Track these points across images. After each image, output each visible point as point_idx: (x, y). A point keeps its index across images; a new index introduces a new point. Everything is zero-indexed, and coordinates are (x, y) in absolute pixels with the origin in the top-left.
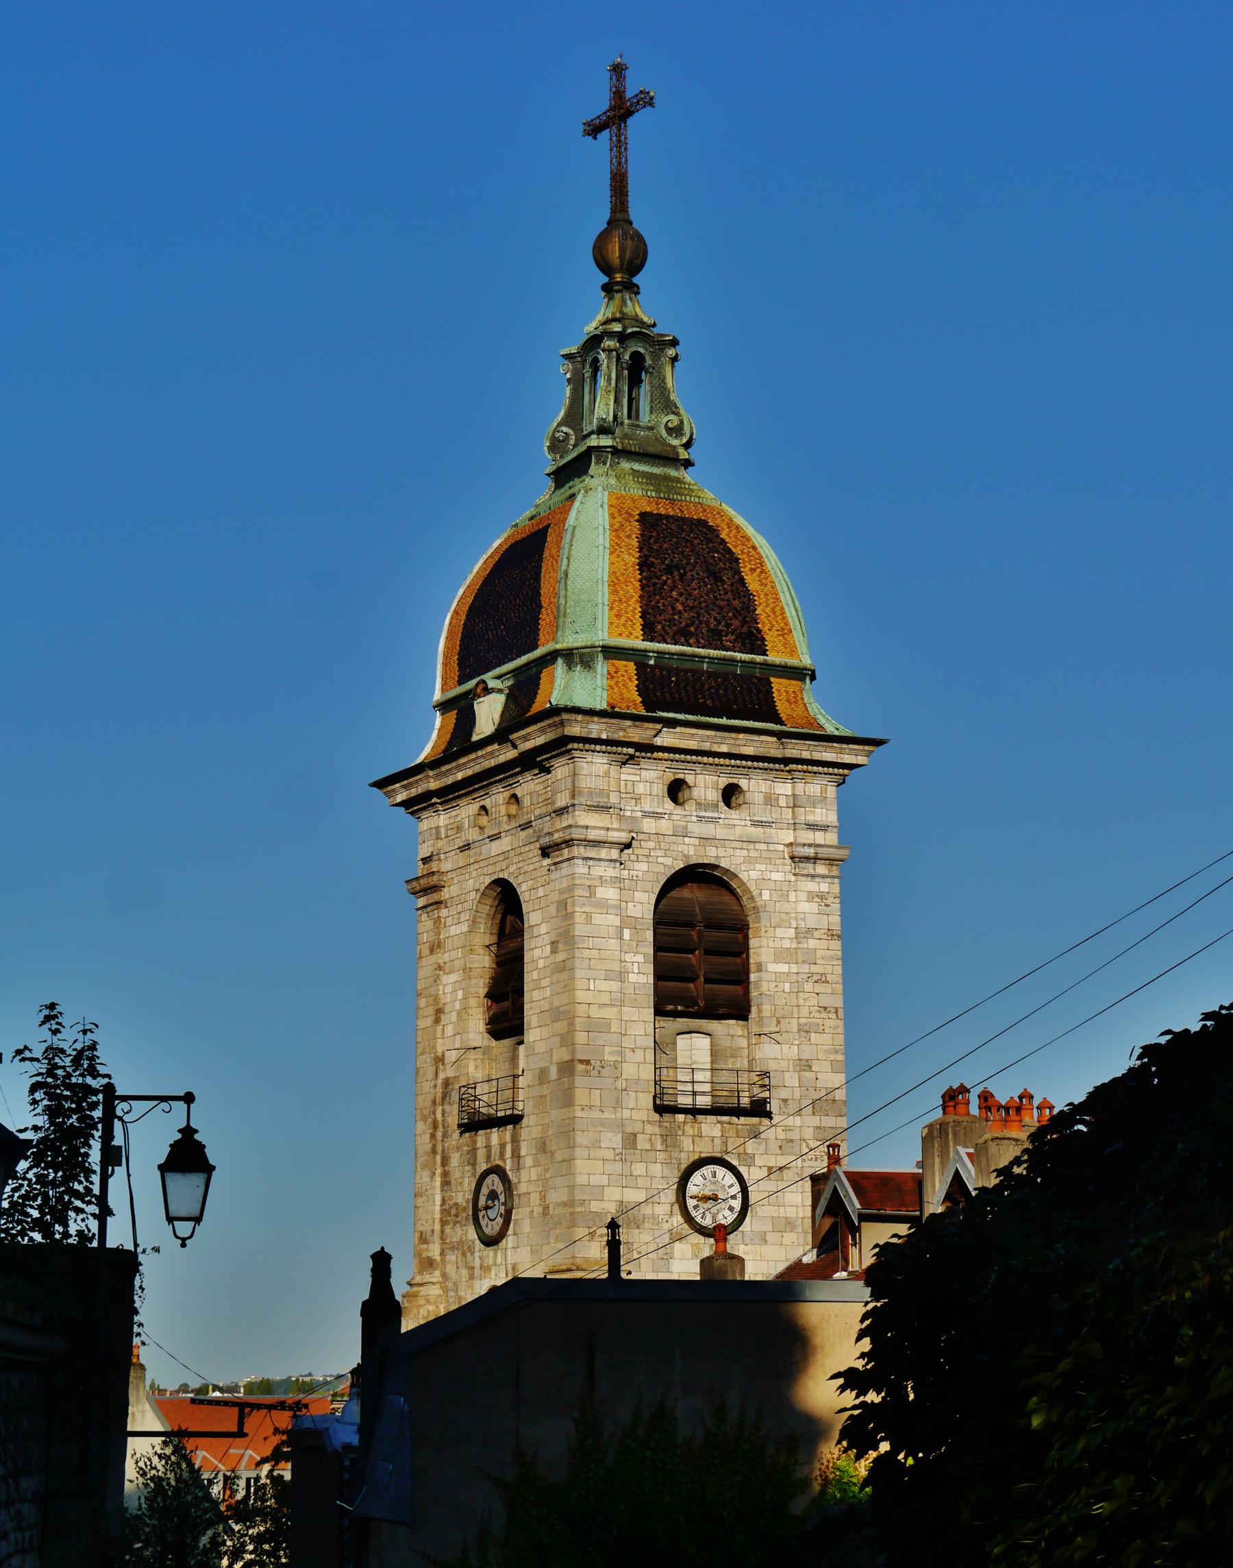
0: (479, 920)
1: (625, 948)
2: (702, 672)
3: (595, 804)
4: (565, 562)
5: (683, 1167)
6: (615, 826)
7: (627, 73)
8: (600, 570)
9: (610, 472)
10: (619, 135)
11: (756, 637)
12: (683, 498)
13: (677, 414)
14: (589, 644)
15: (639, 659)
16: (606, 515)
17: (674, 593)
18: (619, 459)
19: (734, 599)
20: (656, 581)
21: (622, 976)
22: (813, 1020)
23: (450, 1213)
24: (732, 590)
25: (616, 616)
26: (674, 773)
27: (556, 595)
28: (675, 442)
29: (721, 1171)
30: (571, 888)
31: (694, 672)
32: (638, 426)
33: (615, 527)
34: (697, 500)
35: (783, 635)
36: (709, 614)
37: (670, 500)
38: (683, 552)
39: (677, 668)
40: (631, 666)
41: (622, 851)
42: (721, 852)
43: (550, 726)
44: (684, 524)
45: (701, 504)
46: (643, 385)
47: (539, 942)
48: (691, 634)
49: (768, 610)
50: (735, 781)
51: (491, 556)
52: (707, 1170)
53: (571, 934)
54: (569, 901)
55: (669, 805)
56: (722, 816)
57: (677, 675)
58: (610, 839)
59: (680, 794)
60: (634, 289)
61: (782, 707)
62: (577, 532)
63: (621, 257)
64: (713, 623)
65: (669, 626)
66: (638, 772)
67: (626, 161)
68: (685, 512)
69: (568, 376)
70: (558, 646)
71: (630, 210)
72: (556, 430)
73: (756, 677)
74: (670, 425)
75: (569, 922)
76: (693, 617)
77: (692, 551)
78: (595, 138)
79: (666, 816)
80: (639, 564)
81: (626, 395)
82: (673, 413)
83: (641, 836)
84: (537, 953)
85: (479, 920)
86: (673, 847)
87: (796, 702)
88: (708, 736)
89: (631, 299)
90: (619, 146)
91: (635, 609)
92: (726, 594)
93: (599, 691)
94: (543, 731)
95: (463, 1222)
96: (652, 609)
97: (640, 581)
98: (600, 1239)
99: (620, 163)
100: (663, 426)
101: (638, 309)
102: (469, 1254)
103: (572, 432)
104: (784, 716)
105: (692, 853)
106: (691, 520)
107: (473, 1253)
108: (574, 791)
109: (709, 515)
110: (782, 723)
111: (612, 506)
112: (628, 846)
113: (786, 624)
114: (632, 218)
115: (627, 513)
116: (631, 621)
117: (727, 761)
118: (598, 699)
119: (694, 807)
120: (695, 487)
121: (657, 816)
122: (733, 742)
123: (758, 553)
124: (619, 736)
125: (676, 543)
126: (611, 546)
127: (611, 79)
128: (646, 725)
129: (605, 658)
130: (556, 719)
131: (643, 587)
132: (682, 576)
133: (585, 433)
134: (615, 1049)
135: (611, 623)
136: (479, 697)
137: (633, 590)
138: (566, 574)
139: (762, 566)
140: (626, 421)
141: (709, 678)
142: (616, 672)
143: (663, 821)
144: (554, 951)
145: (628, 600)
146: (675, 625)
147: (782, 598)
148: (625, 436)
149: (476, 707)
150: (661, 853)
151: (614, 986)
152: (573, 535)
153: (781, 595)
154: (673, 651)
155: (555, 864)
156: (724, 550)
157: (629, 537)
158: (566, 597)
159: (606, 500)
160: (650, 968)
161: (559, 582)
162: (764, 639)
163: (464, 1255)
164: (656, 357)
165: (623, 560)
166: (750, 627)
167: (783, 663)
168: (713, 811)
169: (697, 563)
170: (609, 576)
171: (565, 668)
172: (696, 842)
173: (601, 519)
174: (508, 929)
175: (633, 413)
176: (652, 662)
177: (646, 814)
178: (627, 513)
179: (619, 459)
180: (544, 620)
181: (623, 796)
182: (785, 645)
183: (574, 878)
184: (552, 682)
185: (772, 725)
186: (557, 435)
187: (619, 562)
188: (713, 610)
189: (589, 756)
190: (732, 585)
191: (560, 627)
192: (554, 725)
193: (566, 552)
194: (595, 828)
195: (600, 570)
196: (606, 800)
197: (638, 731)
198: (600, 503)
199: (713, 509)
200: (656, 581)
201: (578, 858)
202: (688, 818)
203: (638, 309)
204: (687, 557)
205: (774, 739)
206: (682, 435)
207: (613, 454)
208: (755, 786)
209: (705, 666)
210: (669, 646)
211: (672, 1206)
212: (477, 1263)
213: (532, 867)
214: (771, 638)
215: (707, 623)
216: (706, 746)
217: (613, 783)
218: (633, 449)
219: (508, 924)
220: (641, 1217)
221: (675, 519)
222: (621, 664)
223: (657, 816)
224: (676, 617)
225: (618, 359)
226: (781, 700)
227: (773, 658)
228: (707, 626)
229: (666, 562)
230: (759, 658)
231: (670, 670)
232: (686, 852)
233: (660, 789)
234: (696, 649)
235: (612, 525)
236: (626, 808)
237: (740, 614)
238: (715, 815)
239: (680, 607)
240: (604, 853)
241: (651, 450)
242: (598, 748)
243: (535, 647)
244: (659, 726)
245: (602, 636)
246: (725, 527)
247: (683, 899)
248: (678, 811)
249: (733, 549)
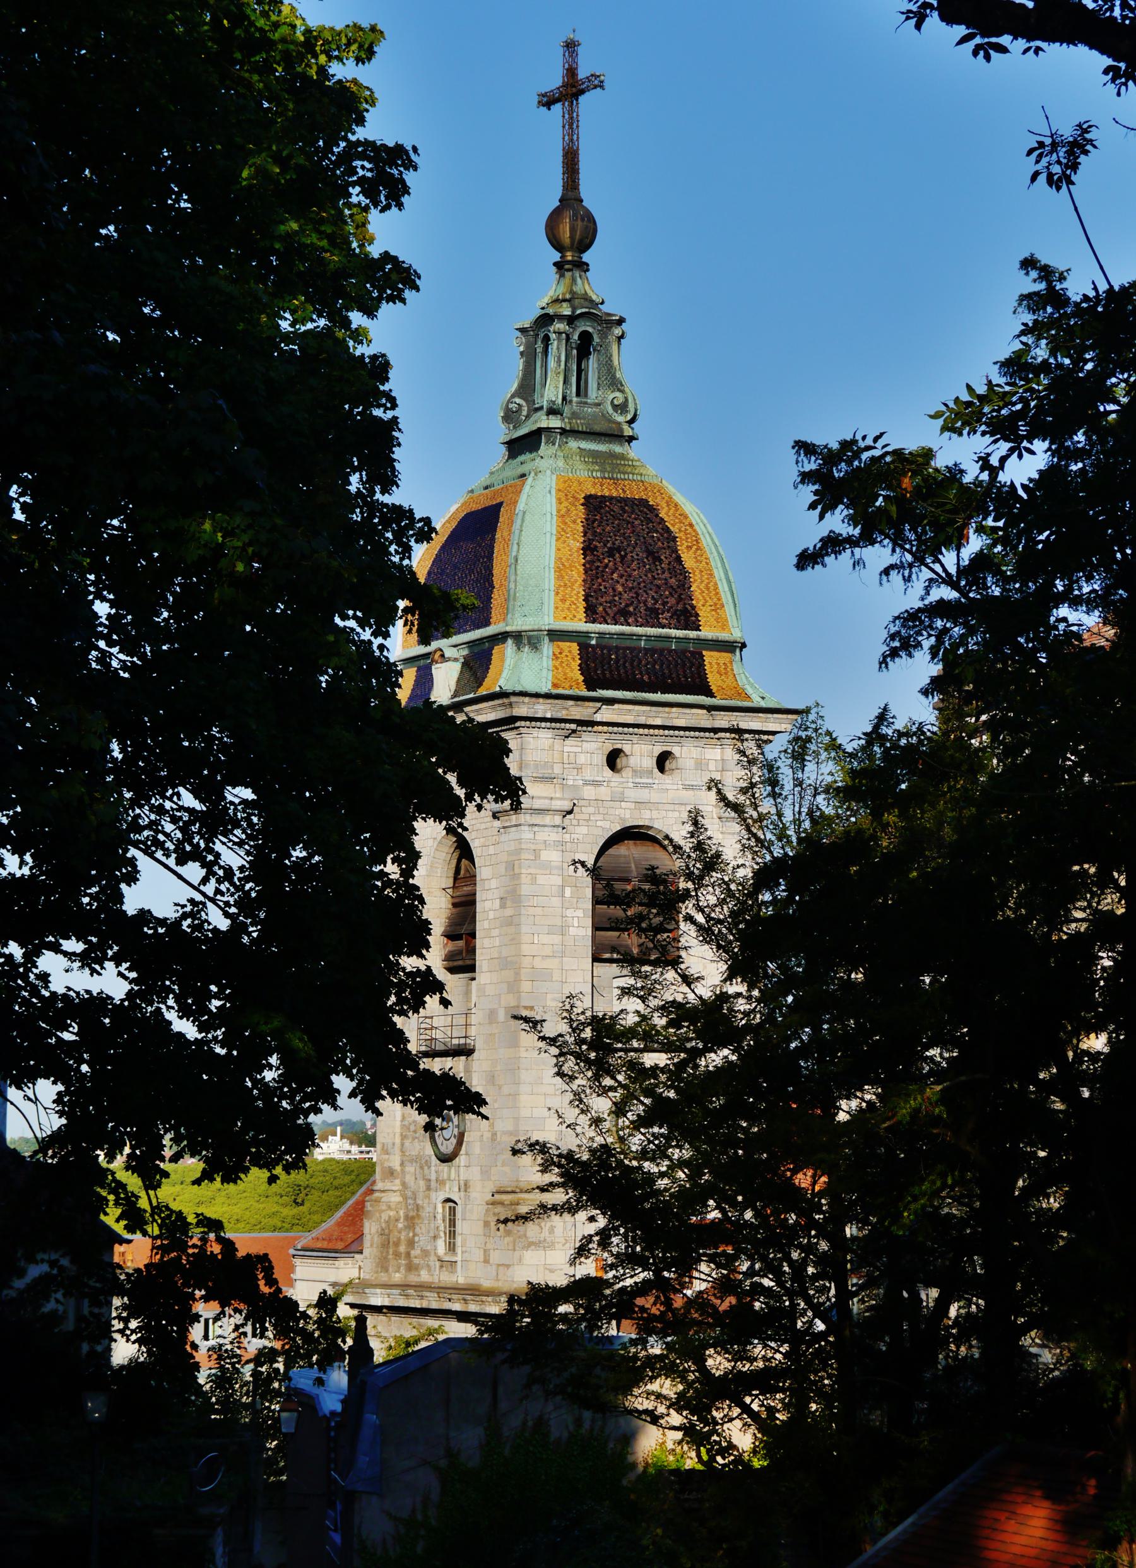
0: (437, 865)
1: (566, 905)
2: (640, 649)
3: (541, 776)
4: (515, 547)
6: (558, 795)
7: (580, 49)
8: (547, 557)
9: (558, 453)
10: (571, 112)
11: (690, 613)
12: (626, 476)
13: (622, 392)
14: (536, 627)
15: (582, 640)
16: (554, 500)
17: (615, 575)
18: (567, 438)
19: (671, 578)
20: (599, 564)
21: (563, 930)
23: (409, 1129)
24: (669, 569)
25: (561, 600)
26: (613, 744)
27: (507, 578)
28: (620, 419)
30: (519, 851)
31: (632, 649)
32: (586, 403)
33: (562, 512)
34: (639, 478)
35: (715, 610)
36: (647, 594)
37: (614, 479)
38: (624, 534)
39: (616, 646)
40: (575, 647)
41: (564, 816)
42: (655, 814)
43: (500, 705)
44: (626, 505)
45: (642, 482)
46: (591, 357)
47: (490, 895)
48: (630, 614)
49: (702, 586)
50: (668, 749)
51: (448, 521)
53: (518, 893)
54: (516, 862)
55: (608, 772)
56: (656, 781)
57: (616, 654)
58: (553, 808)
59: (618, 760)
60: (583, 267)
61: (713, 680)
62: (527, 517)
63: (572, 237)
64: (650, 602)
65: (610, 607)
66: (580, 744)
67: (578, 138)
68: (628, 492)
69: (522, 349)
70: (508, 629)
71: (580, 187)
72: (510, 401)
73: (690, 652)
74: (616, 402)
75: (516, 882)
76: (632, 597)
77: (633, 532)
78: (549, 109)
79: (605, 784)
80: (583, 549)
81: (575, 374)
82: (619, 390)
83: (582, 803)
84: (488, 904)
85: (437, 865)
86: (611, 811)
87: (726, 673)
89: (580, 276)
90: (571, 124)
91: (579, 593)
92: (663, 573)
93: (545, 672)
94: (493, 708)
95: (421, 1138)
96: (595, 592)
97: (584, 565)
99: (571, 140)
100: (609, 403)
101: (587, 287)
102: (426, 1168)
103: (524, 403)
104: (714, 688)
105: (628, 816)
106: (633, 500)
107: (429, 1167)
108: (521, 764)
109: (650, 494)
110: (710, 694)
111: (559, 490)
112: (570, 812)
113: (719, 599)
114: (583, 195)
115: (574, 497)
116: (575, 604)
117: (661, 732)
118: (544, 680)
119: (630, 774)
120: (638, 464)
121: (596, 784)
122: (666, 715)
123: (695, 531)
124: (563, 714)
125: (618, 525)
126: (558, 532)
127: (564, 55)
128: (587, 704)
129: (551, 640)
130: (506, 701)
131: (586, 572)
132: (623, 558)
133: (537, 406)
134: (556, 995)
135: (557, 608)
136: (437, 663)
137: (577, 575)
138: (516, 560)
139: (698, 543)
140: (575, 399)
141: (646, 654)
142: (560, 653)
143: (602, 788)
144: (503, 906)
145: (573, 585)
146: (615, 606)
147: (716, 574)
148: (574, 415)
149: (434, 671)
150: (600, 817)
151: (557, 939)
152: (523, 521)
153: (715, 571)
154: (613, 631)
155: (504, 828)
156: (663, 529)
157: (574, 522)
158: (515, 581)
159: (554, 485)
160: (589, 922)
161: (510, 566)
162: (697, 615)
163: (422, 1168)
164: (604, 335)
165: (568, 546)
166: (685, 604)
167: (714, 638)
168: (648, 778)
169: (637, 544)
170: (556, 563)
171: (515, 648)
172: (632, 806)
173: (548, 505)
174: (462, 872)
175: (582, 392)
176: (593, 642)
177: (586, 783)
178: (574, 497)
179: (567, 438)
180: (496, 600)
181: (566, 766)
182: (717, 620)
183: (520, 843)
184: (503, 660)
185: (703, 697)
186: (511, 406)
187: (564, 548)
188: (651, 589)
189: (535, 732)
190: (669, 563)
191: (510, 610)
192: (503, 705)
193: (516, 538)
194: (539, 798)
195: (547, 557)
196: (550, 771)
197: (579, 709)
198: (548, 489)
199: (653, 486)
200: (599, 564)
201: (524, 825)
202: (625, 785)
203: (587, 287)
204: (628, 539)
205: (705, 711)
206: (627, 411)
207: (561, 434)
208: (686, 752)
209: (643, 643)
210: (610, 626)
212: (433, 1177)
213: (483, 826)
214: (705, 614)
215: (645, 602)
216: (642, 720)
217: (556, 755)
218: (580, 429)
219: (463, 867)
221: (619, 500)
222: (565, 645)
223: (596, 784)
224: (617, 598)
225: (568, 338)
226: (712, 672)
227: (706, 633)
228: (645, 605)
229: (609, 545)
230: (692, 634)
231: (610, 649)
232: (622, 816)
233: (602, 759)
234: (635, 628)
235: (559, 511)
236: (569, 777)
237: (676, 592)
238: (650, 781)
239: (620, 588)
240: (547, 819)
241: (597, 428)
242: (543, 724)
243: (487, 623)
244: (598, 705)
245: (549, 621)
246: (665, 505)
247: (619, 856)
248: (614, 778)
249: (671, 528)
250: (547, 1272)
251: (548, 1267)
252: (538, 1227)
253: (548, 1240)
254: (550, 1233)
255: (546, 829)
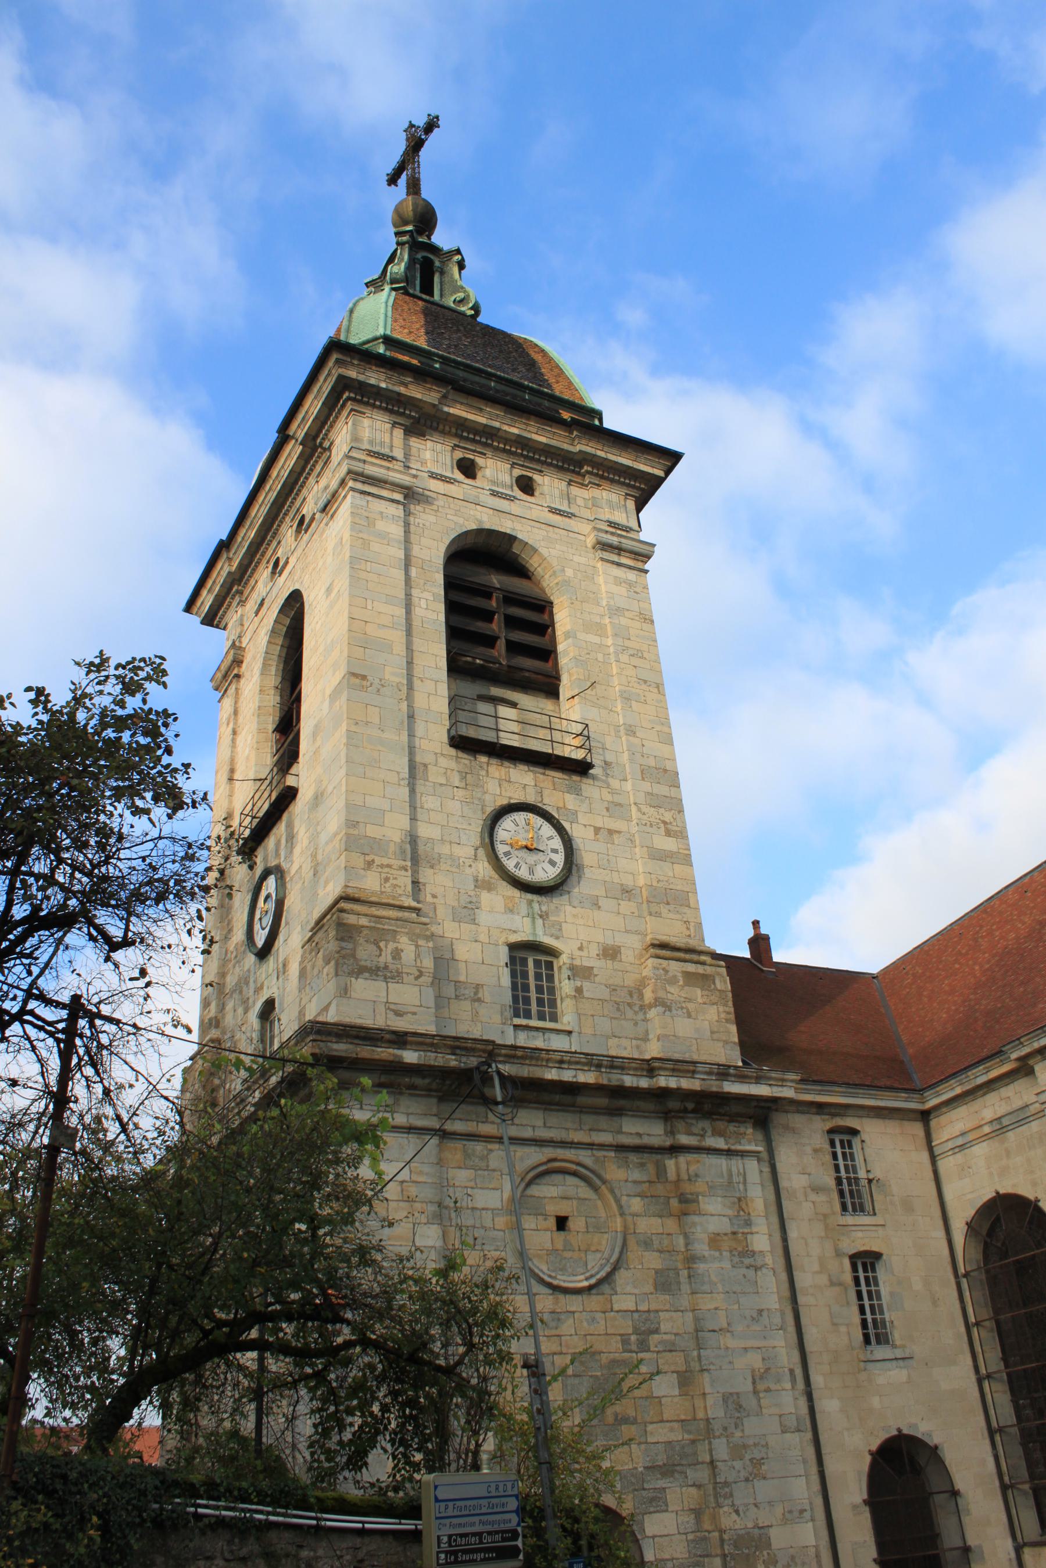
5: (489, 810)
22: (634, 690)
29: (537, 820)
52: (521, 817)
88: (497, 415)
98: (380, 870)
160: (442, 607)
211: (476, 849)
220: (436, 856)
250: (391, 1015)
251: (392, 1007)
252: (374, 948)
253: (391, 966)
254: (394, 958)
255: (383, 502)
